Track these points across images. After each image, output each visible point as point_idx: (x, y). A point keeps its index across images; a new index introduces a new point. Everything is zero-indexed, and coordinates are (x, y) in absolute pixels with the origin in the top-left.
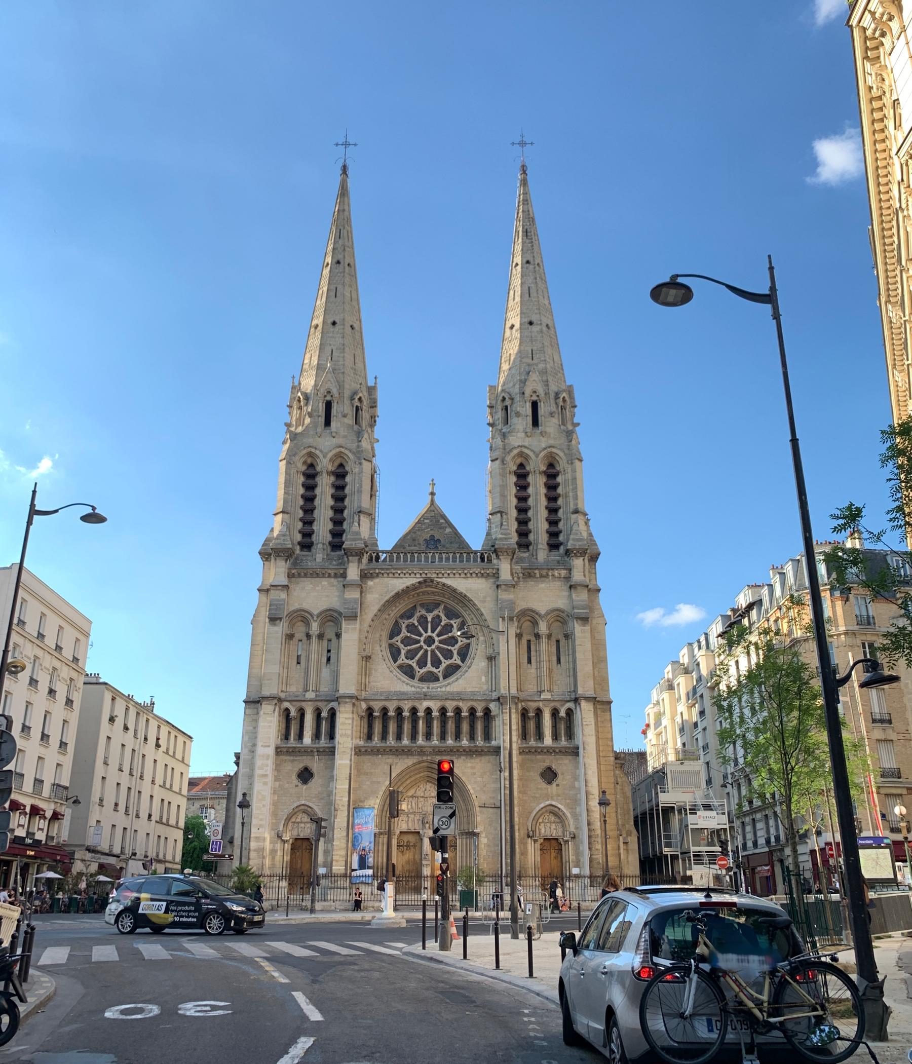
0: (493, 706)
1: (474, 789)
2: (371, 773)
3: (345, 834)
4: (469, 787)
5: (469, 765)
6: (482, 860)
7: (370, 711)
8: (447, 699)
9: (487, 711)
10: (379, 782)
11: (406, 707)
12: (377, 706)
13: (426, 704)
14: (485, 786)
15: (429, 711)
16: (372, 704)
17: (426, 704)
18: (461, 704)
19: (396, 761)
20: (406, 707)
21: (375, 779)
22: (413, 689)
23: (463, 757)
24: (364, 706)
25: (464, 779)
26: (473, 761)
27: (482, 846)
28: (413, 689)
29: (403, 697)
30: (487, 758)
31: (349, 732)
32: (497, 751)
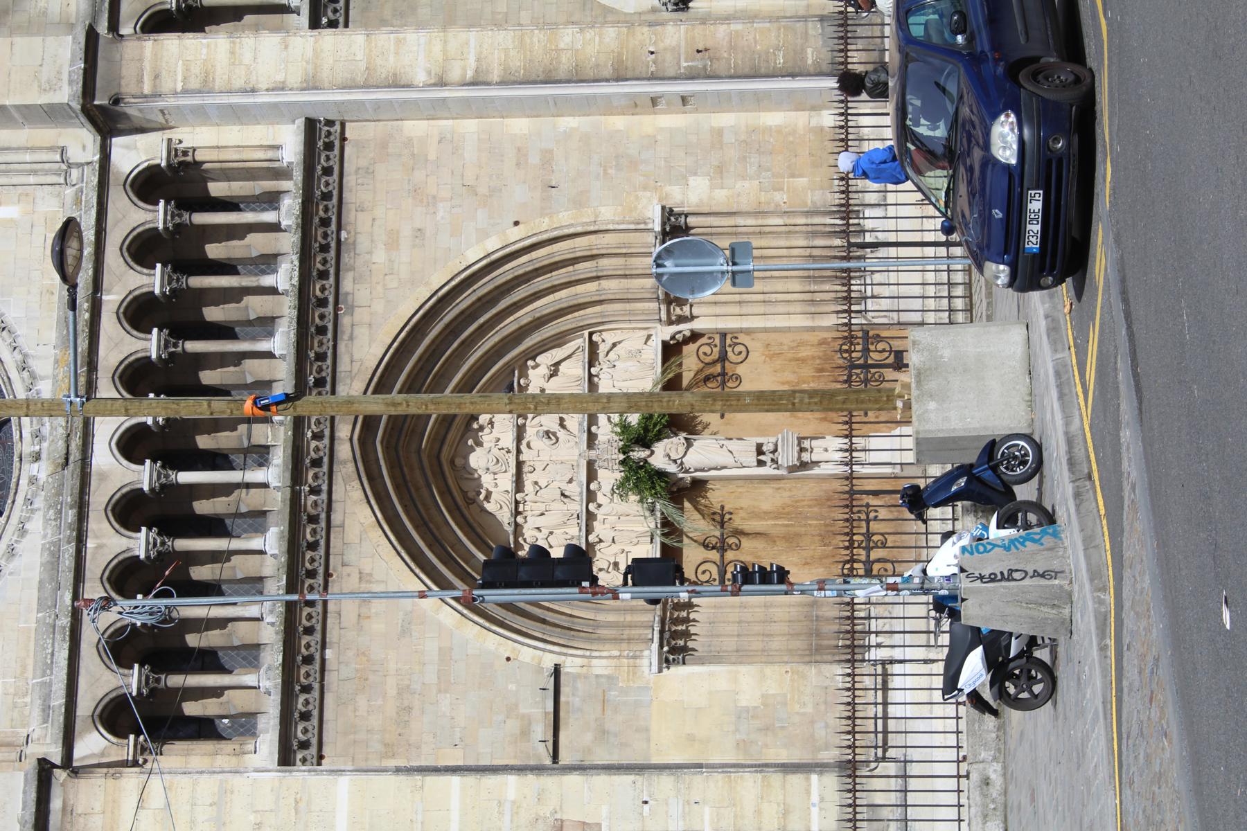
0: (131, 154)
1: (484, 235)
2: (403, 691)
3: (665, 782)
4: (473, 254)
5: (380, 256)
6: (780, 198)
7: (115, 717)
8: (92, 366)
9: (148, 185)
10: (445, 655)
11: (110, 543)
12: (102, 680)
13: (104, 456)
14: (471, 189)
15: (133, 445)
16: (86, 705)
17: (104, 456)
18: (112, 299)
19: (351, 583)
20: (110, 543)
21: (431, 677)
22: (36, 525)
23: (347, 284)
24: (93, 743)
25: (438, 278)
26: (363, 243)
27: (721, 198)
28: (36, 525)
29: (68, 561)
30: (349, 180)
31: (208, 785)
32: (322, 139)
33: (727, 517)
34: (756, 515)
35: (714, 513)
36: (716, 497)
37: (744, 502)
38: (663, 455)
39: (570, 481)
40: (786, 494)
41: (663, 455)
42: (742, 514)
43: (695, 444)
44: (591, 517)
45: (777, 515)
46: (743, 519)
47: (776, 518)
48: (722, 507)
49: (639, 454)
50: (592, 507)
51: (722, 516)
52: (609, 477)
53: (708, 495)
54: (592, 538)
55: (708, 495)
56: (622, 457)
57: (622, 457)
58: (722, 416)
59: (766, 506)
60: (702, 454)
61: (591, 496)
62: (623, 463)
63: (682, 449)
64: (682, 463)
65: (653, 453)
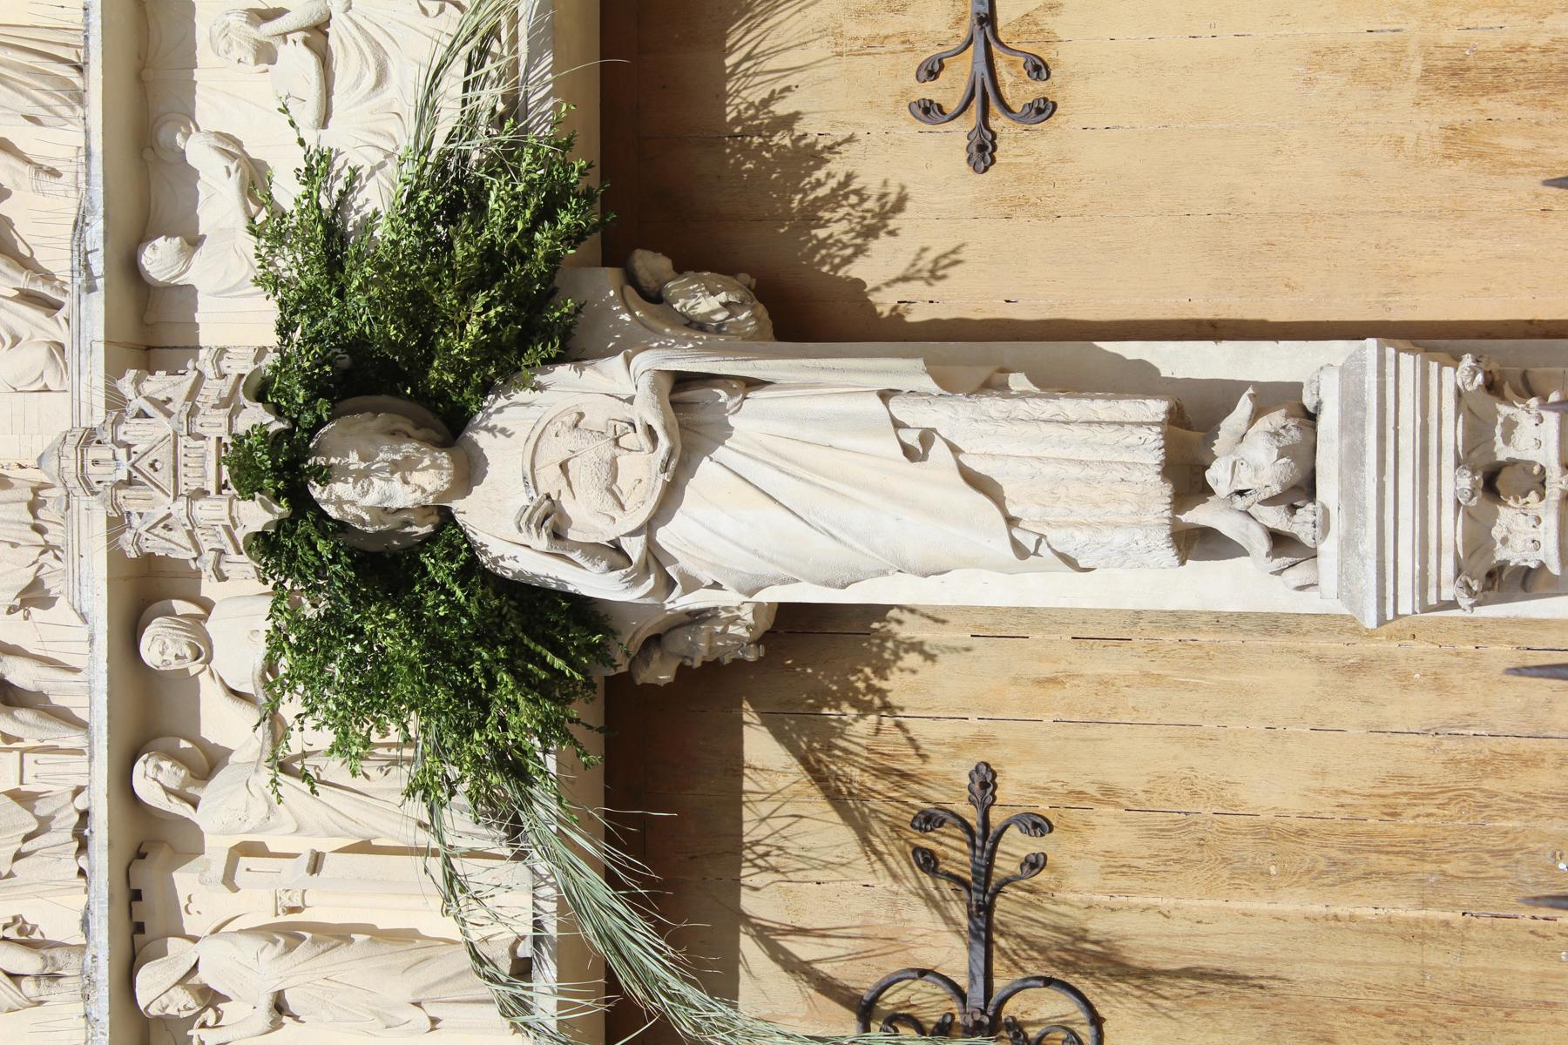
33: (1015, 847)
34: (1204, 839)
35: (929, 820)
36: (936, 715)
37: (1128, 758)
38: (554, 471)
39: (34, 596)
40: (1417, 708)
41: (554, 471)
42: (1111, 831)
43: (749, 421)
44: (148, 847)
45: (1341, 848)
46: (1117, 866)
47: (1338, 874)
48: (985, 782)
49: (377, 484)
50: (153, 781)
51: (985, 839)
52: (241, 616)
53: (896, 685)
54: (156, 987)
55: (896, 685)
56: (256, 515)
57: (256, 515)
58: (983, 152)
59: (1272, 787)
60: (781, 492)
61: (151, 715)
62: (266, 545)
63: (642, 470)
64: (652, 549)
65: (470, 472)
